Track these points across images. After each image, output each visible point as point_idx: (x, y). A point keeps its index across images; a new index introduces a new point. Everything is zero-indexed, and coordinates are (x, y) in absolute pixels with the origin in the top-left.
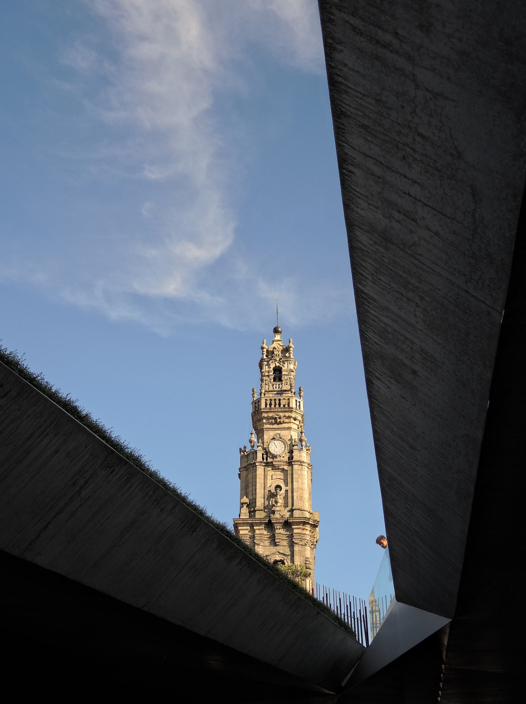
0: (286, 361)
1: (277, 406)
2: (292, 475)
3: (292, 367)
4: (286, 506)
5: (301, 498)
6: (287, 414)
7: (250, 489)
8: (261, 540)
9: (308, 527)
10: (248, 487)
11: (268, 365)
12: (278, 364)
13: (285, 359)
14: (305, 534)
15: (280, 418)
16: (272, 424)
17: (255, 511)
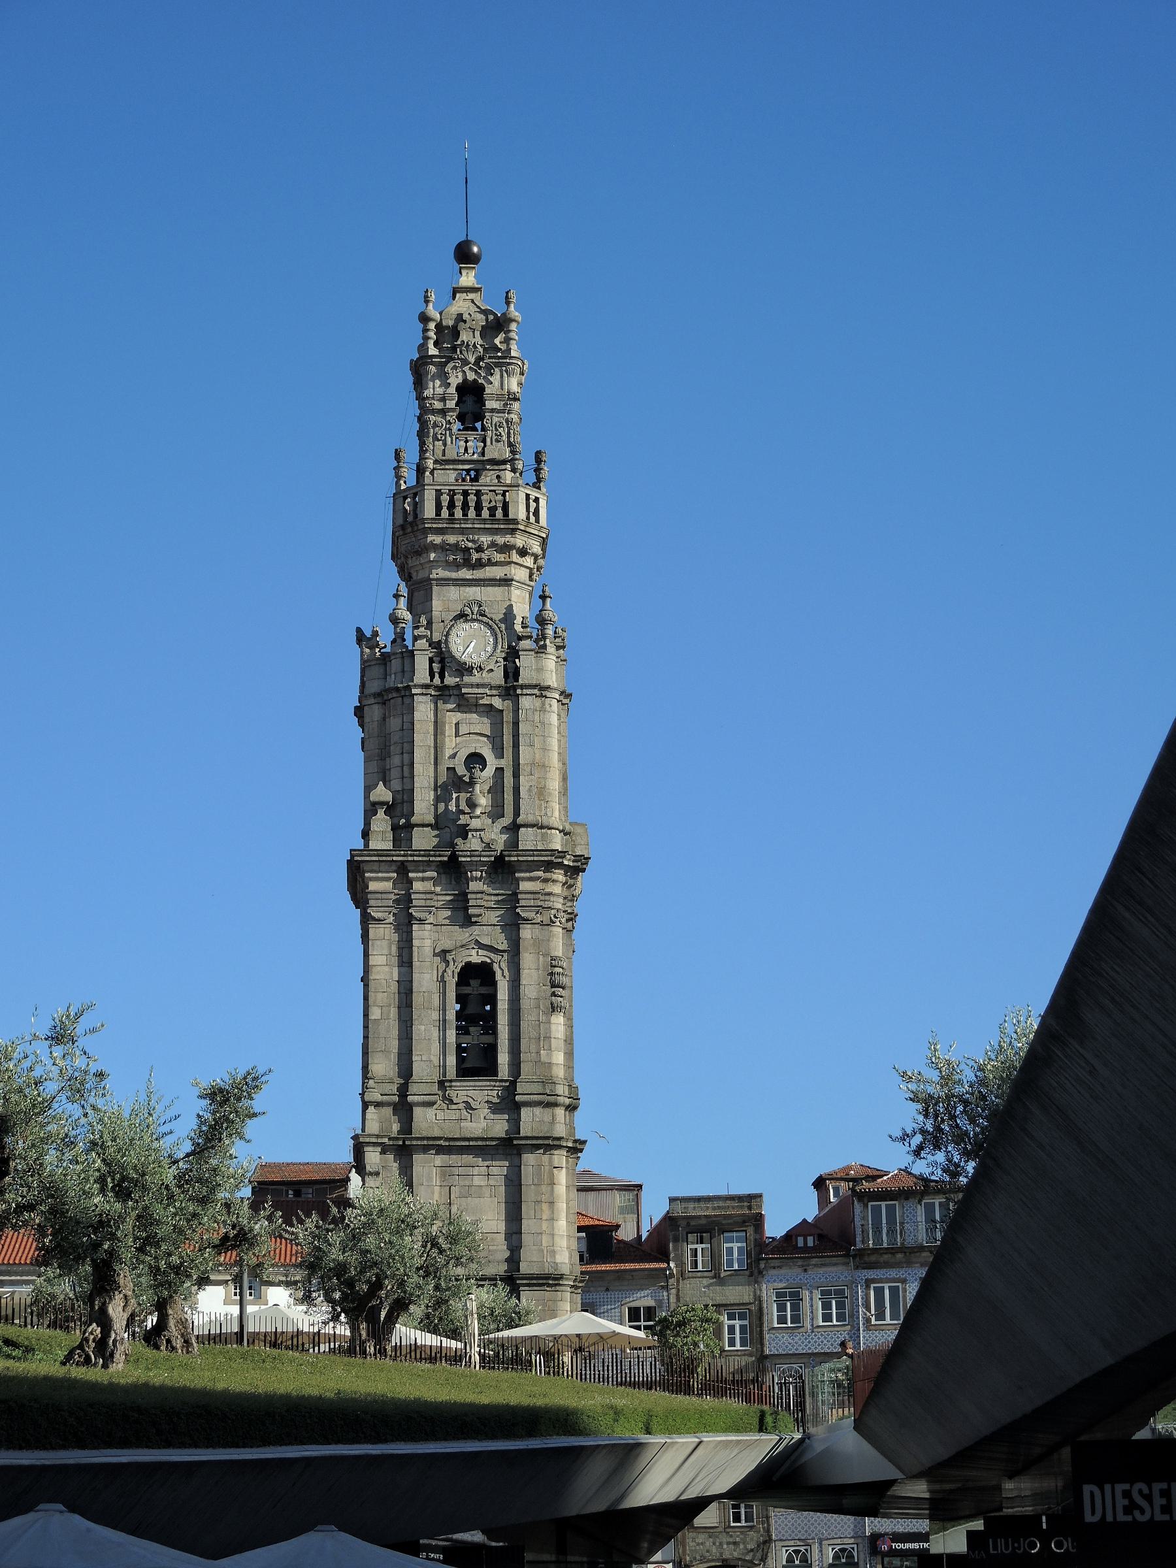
0: (498, 365)
1: (472, 513)
2: (516, 724)
3: (513, 385)
4: (496, 812)
5: (541, 793)
6: (500, 540)
7: (396, 760)
8: (428, 909)
9: (559, 875)
10: (386, 753)
11: (444, 377)
12: (471, 376)
13: (498, 360)
14: (550, 894)
15: (479, 549)
16: (457, 566)
17: (410, 827)
